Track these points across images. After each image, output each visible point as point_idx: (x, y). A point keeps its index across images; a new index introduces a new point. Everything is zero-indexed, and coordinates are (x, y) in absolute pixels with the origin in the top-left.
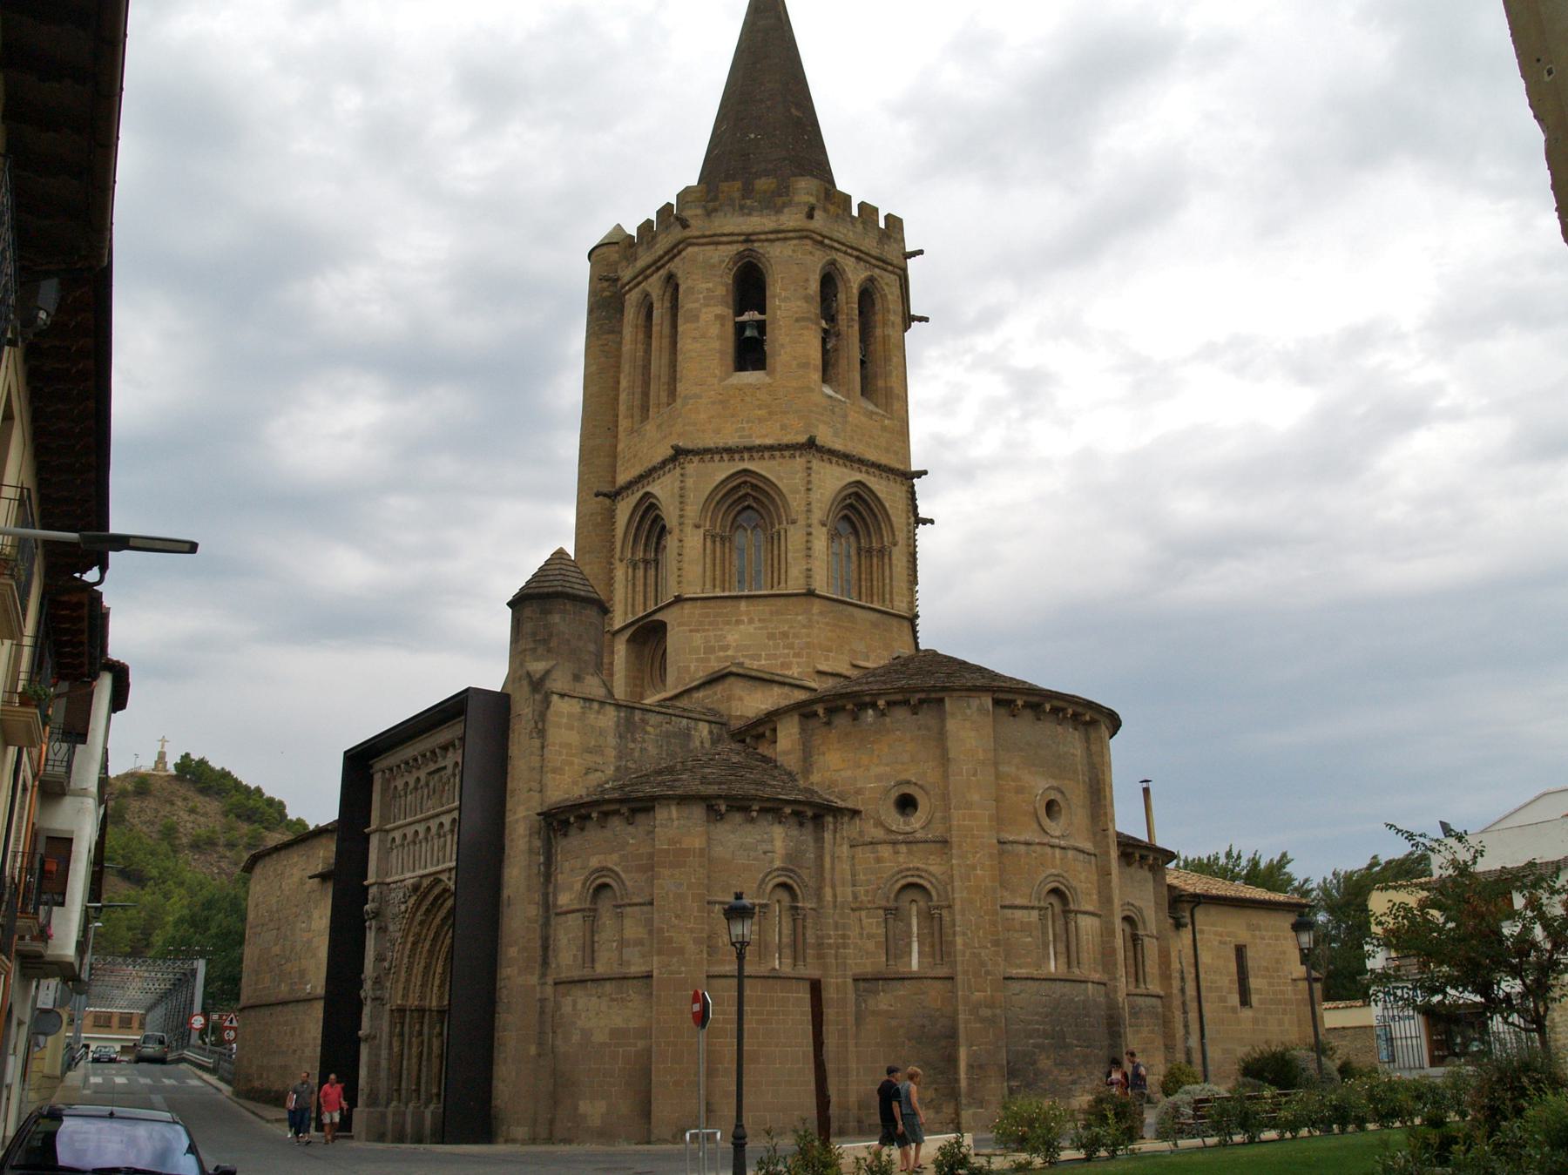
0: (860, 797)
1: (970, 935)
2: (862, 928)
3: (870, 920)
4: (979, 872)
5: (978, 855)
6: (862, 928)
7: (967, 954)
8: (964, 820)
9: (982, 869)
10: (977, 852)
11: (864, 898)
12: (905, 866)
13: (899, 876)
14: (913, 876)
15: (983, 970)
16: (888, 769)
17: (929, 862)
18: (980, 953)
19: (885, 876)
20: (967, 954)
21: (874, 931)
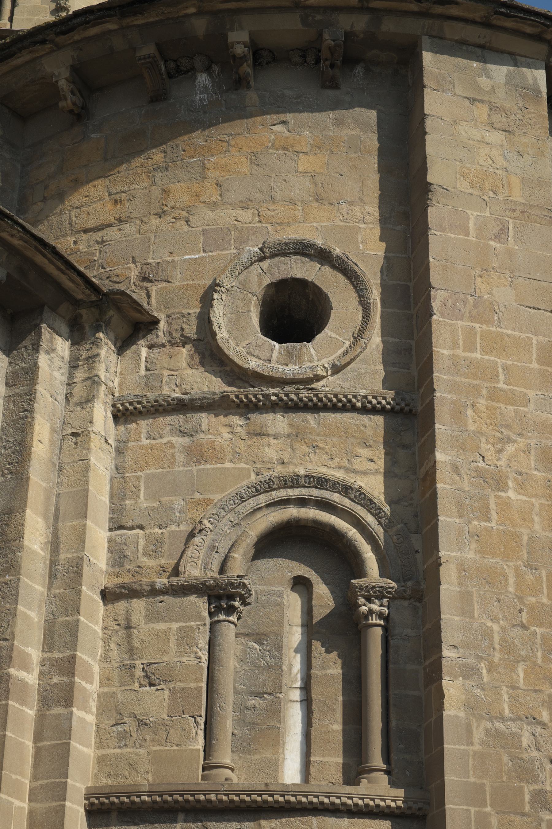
0: (154, 289)
1: (486, 677)
2: (131, 650)
3: (162, 626)
4: (511, 494)
5: (510, 449)
6: (131, 650)
7: (478, 734)
8: (470, 347)
9: (521, 487)
10: (505, 440)
11: (144, 560)
12: (280, 470)
13: (263, 499)
14: (302, 502)
15: (528, 790)
16: (246, 216)
17: (358, 464)
18: (517, 737)
19: (216, 497)
20: (478, 734)
21: (171, 657)
